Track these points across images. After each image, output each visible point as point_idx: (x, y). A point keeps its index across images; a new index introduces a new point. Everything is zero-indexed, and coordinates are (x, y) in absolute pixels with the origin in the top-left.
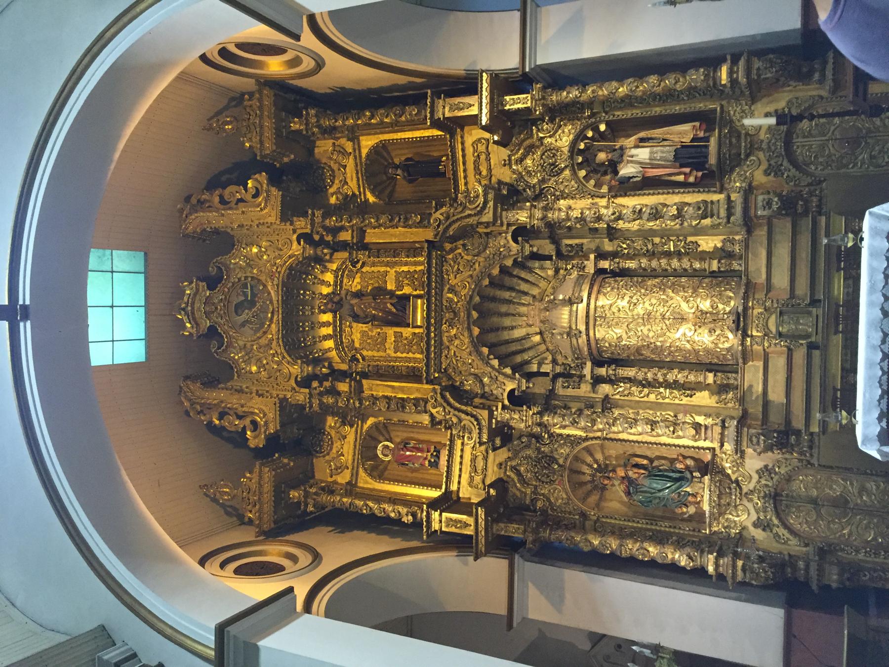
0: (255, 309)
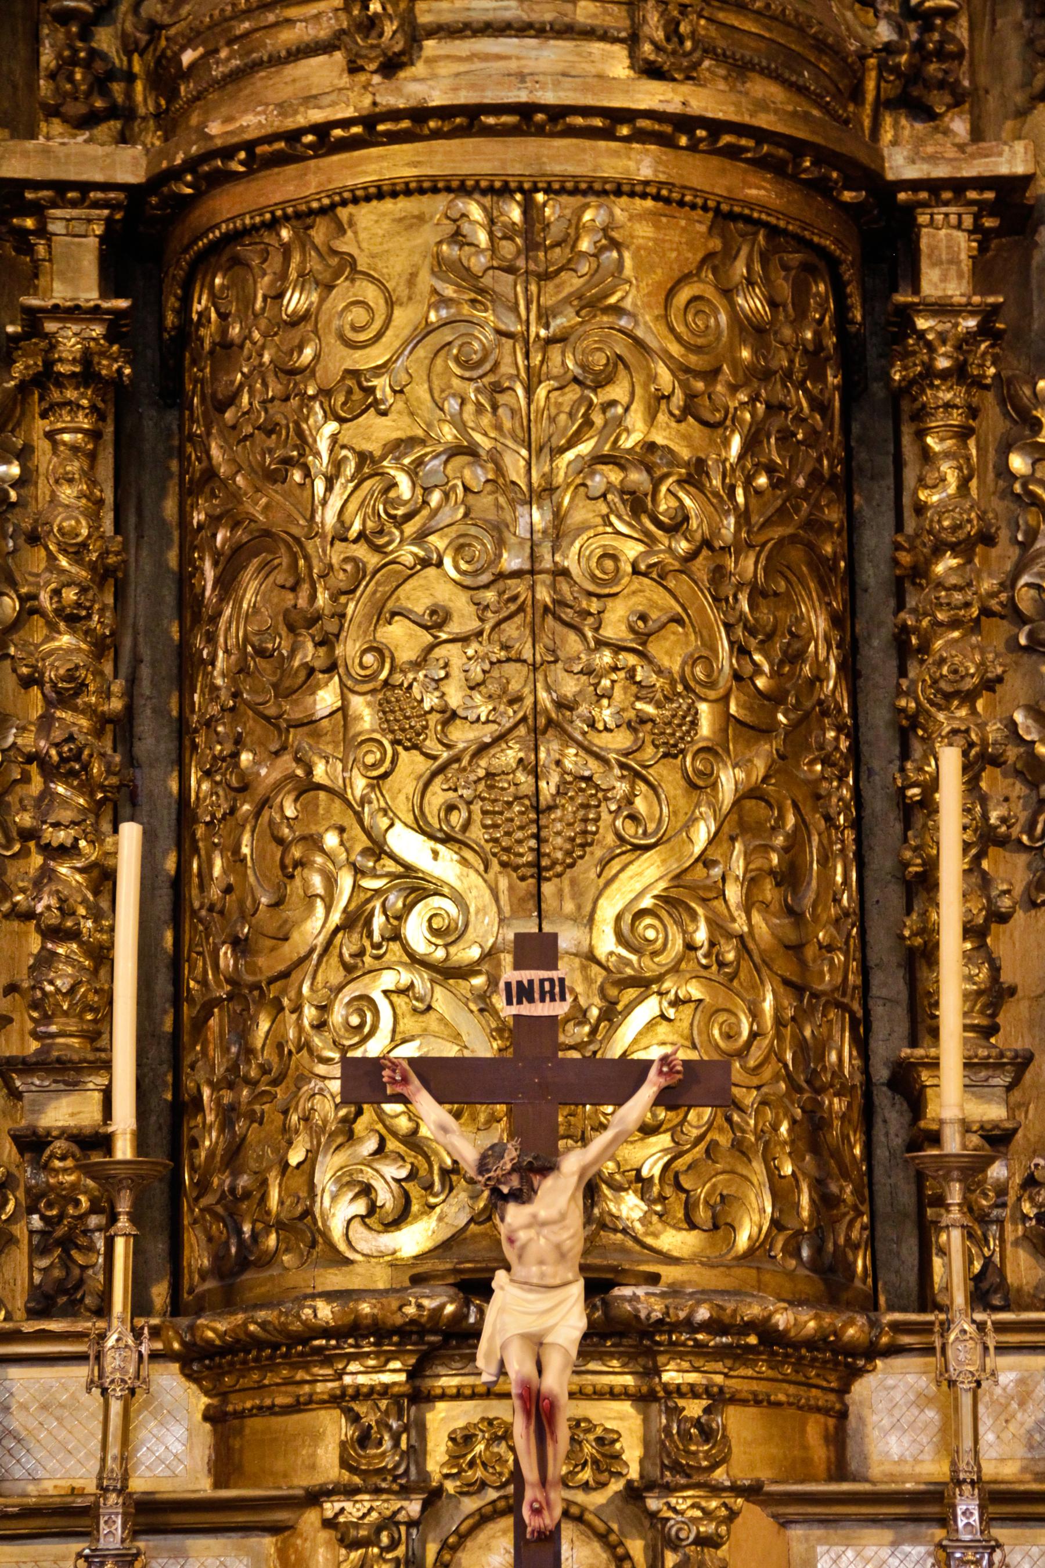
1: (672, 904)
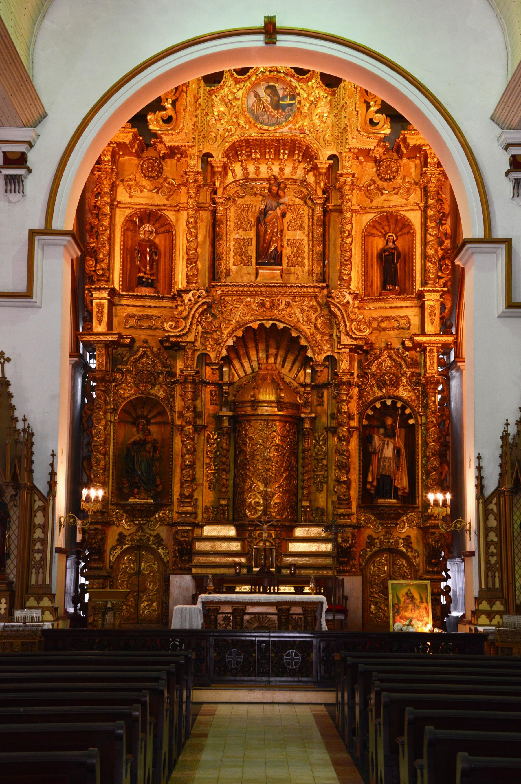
0: (271, 110)
1: (279, 487)
